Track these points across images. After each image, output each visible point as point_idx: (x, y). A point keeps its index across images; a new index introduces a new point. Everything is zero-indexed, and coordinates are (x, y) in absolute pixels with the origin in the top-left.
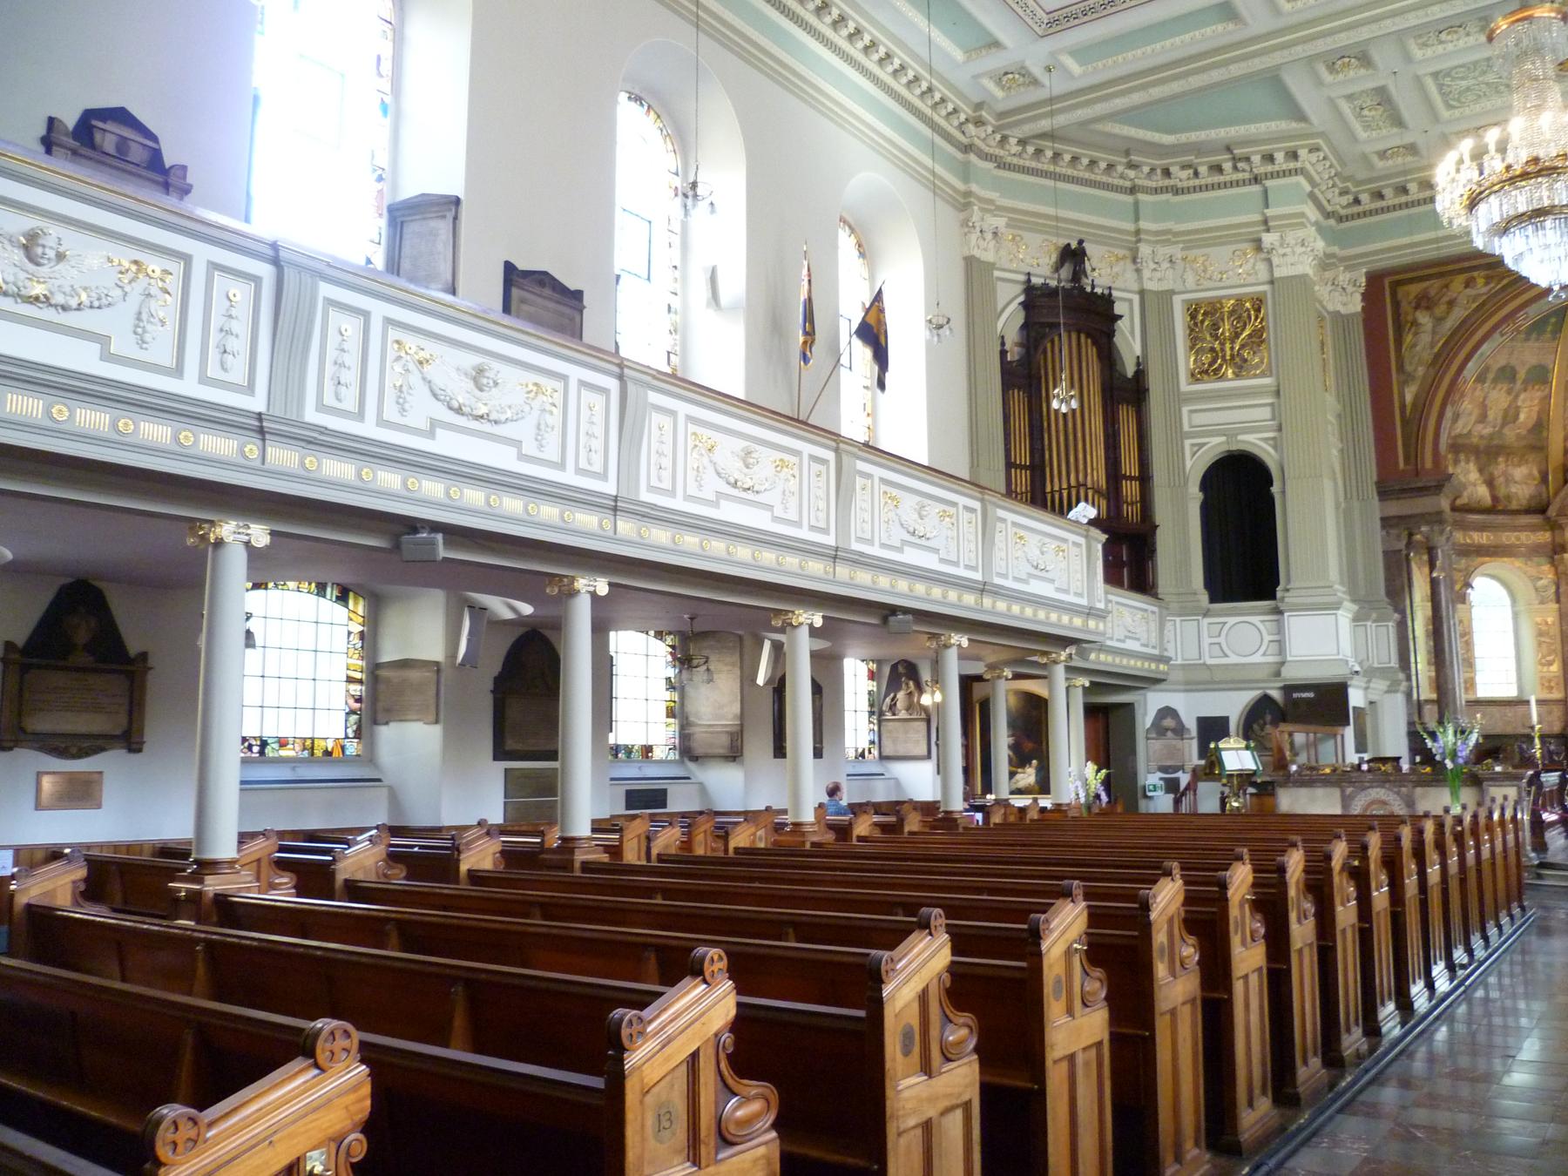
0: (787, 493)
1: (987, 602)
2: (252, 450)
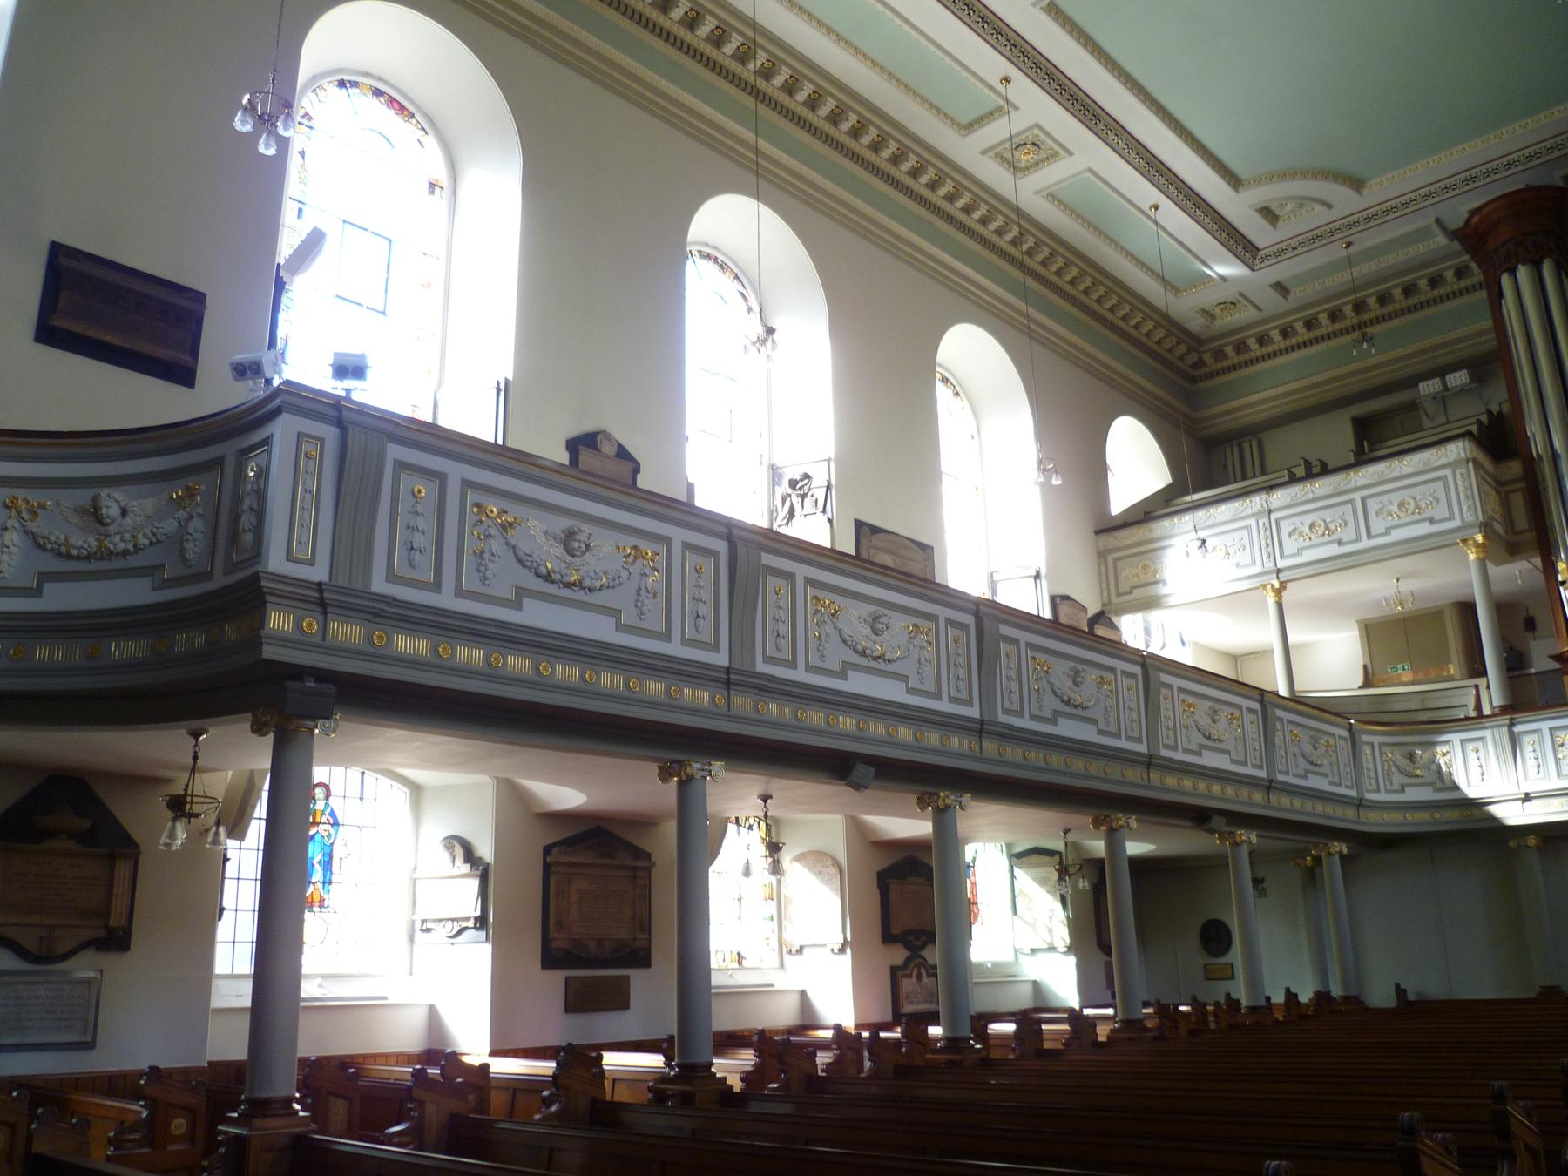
0: (923, 661)
1: (1155, 776)
2: (311, 625)
